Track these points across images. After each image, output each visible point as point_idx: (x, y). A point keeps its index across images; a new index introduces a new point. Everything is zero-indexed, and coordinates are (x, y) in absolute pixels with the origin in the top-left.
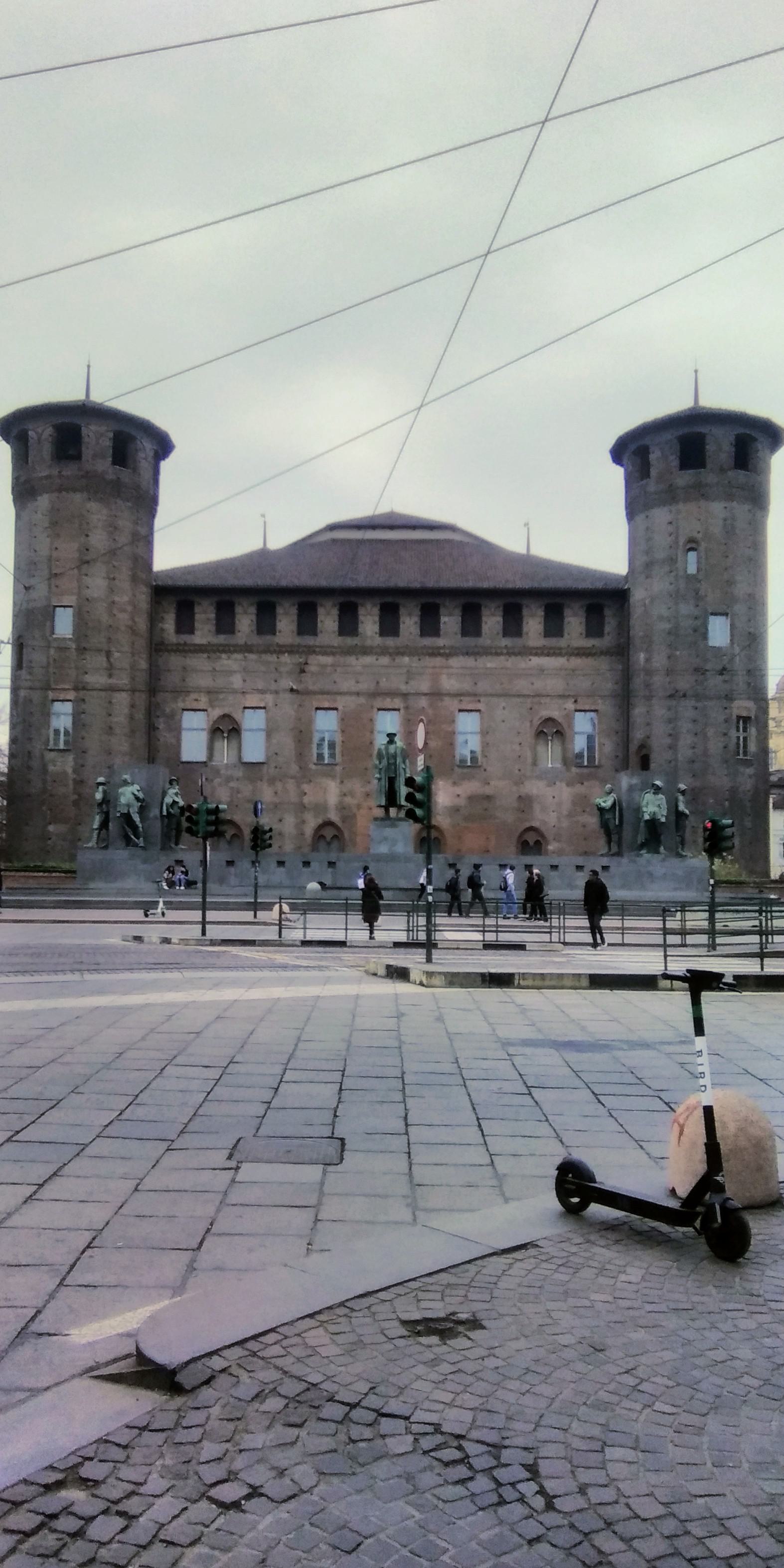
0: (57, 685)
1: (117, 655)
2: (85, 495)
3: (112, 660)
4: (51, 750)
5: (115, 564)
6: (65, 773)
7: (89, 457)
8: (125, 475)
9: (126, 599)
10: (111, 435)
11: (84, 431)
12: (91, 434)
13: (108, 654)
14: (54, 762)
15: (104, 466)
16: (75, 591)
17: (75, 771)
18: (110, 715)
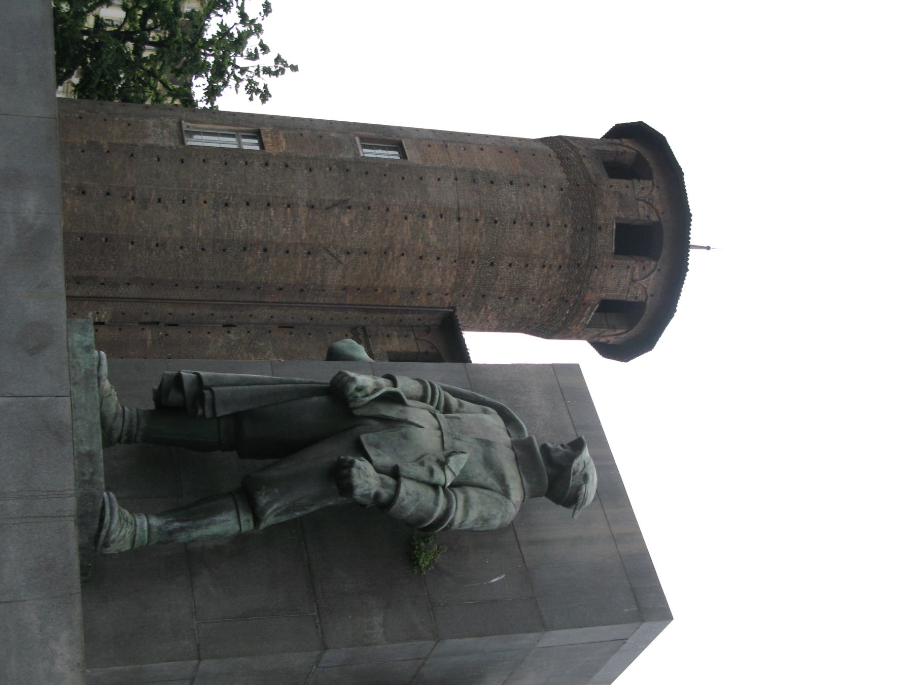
0: (285, 137)
1: (346, 220)
2: (566, 184)
3: (336, 210)
4: (180, 124)
5: (481, 222)
6: (146, 136)
7: (609, 225)
8: (606, 241)
9: (433, 239)
10: (654, 218)
11: (648, 183)
12: (646, 193)
13: (344, 205)
14: (164, 126)
15: (610, 213)
16: (429, 164)
17: (151, 146)
18: (248, 204)
